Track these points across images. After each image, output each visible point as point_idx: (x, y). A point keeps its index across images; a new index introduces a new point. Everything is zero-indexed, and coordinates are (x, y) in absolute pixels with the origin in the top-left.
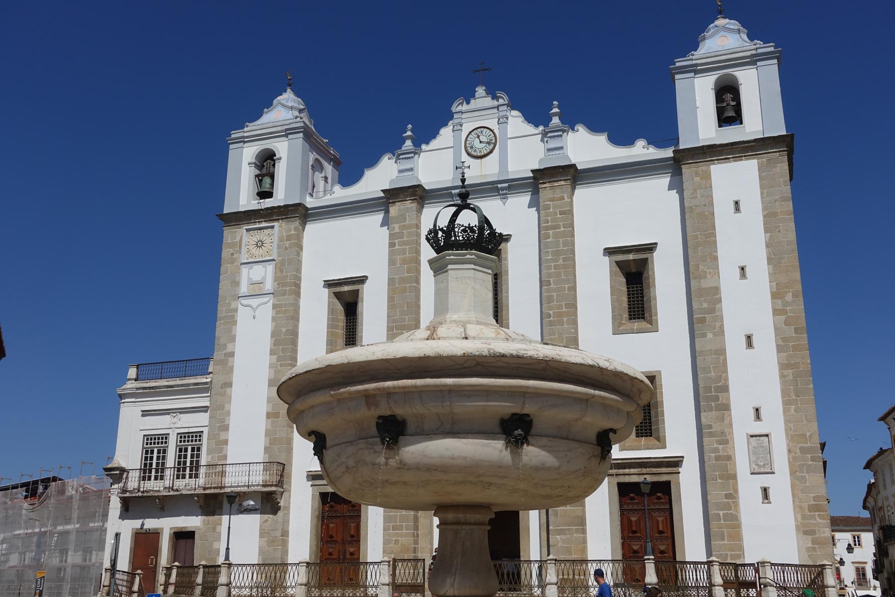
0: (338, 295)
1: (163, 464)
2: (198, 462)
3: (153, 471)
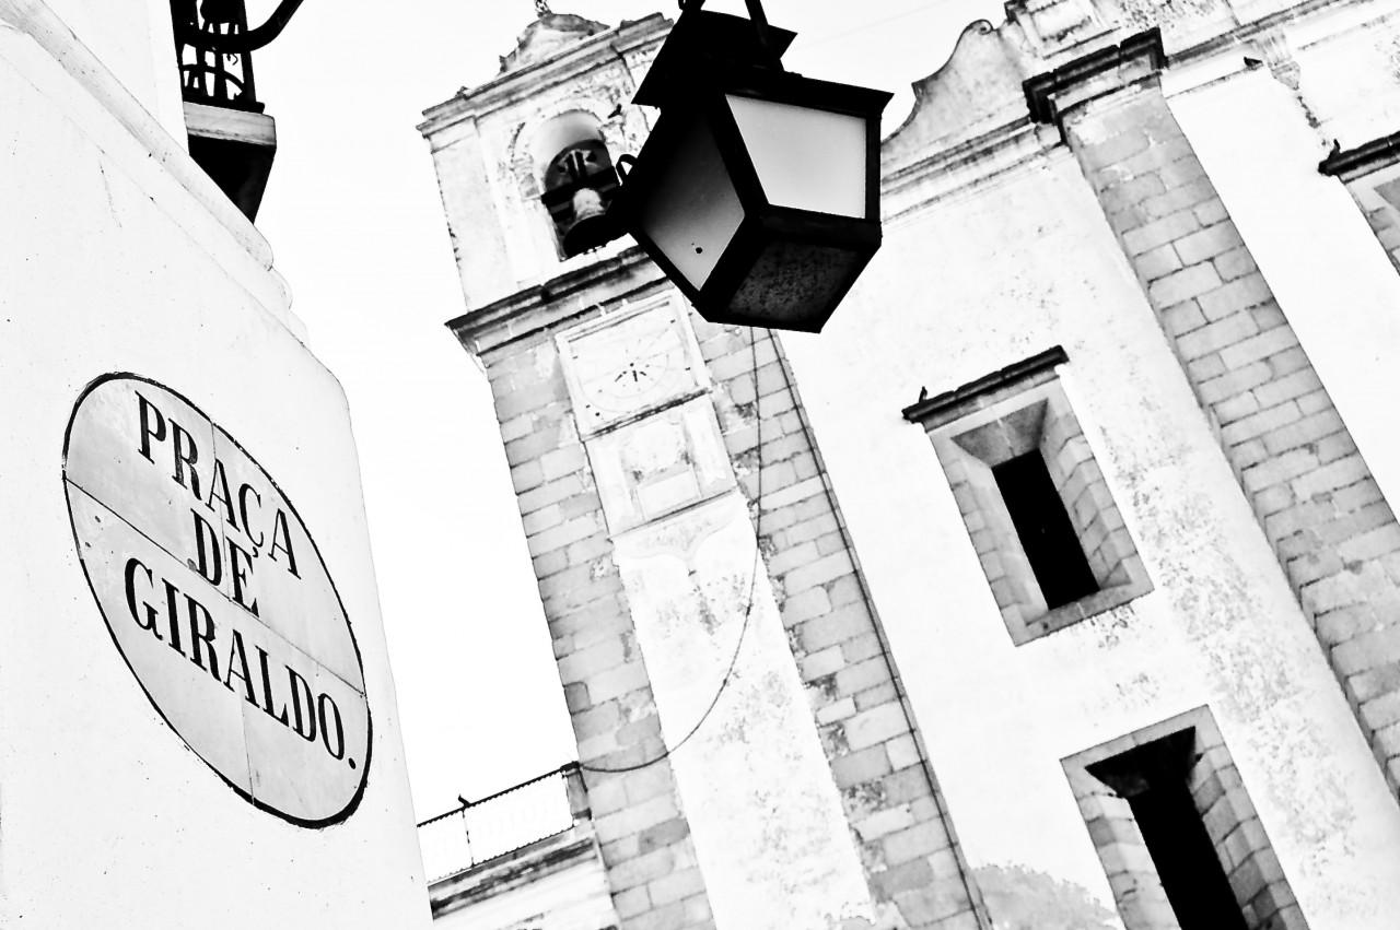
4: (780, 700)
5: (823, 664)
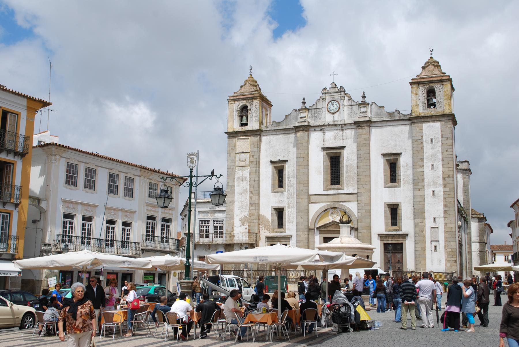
0: (275, 167)
1: (208, 232)
4: (247, 192)
5: (252, 189)
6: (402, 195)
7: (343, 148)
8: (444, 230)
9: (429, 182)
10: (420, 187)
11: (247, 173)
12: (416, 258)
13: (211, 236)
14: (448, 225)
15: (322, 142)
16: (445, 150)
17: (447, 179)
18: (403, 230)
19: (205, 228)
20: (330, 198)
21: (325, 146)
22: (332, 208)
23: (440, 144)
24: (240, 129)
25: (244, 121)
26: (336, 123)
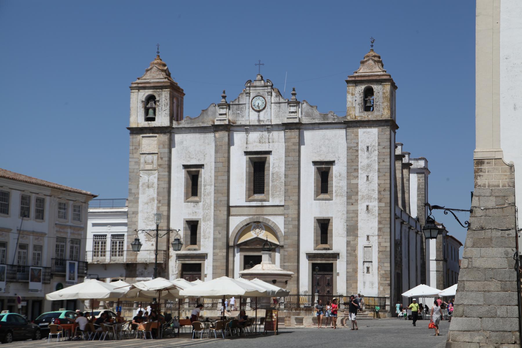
0: (189, 172)
1: (105, 249)
2: (122, 248)
3: (100, 252)
4: (154, 201)
5: (161, 198)
6: (335, 209)
7: (269, 153)
8: (377, 249)
9: (363, 196)
10: (354, 201)
11: (154, 178)
12: (347, 280)
13: (108, 254)
14: (382, 244)
15: (245, 145)
16: (381, 160)
17: (382, 193)
18: (333, 248)
19: (100, 244)
20: (253, 211)
21: (249, 150)
22: (255, 222)
23: (376, 153)
24: (146, 124)
25: (151, 115)
26: (262, 123)
